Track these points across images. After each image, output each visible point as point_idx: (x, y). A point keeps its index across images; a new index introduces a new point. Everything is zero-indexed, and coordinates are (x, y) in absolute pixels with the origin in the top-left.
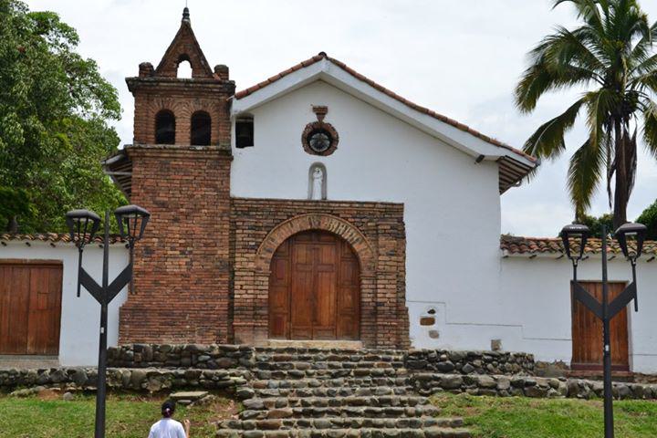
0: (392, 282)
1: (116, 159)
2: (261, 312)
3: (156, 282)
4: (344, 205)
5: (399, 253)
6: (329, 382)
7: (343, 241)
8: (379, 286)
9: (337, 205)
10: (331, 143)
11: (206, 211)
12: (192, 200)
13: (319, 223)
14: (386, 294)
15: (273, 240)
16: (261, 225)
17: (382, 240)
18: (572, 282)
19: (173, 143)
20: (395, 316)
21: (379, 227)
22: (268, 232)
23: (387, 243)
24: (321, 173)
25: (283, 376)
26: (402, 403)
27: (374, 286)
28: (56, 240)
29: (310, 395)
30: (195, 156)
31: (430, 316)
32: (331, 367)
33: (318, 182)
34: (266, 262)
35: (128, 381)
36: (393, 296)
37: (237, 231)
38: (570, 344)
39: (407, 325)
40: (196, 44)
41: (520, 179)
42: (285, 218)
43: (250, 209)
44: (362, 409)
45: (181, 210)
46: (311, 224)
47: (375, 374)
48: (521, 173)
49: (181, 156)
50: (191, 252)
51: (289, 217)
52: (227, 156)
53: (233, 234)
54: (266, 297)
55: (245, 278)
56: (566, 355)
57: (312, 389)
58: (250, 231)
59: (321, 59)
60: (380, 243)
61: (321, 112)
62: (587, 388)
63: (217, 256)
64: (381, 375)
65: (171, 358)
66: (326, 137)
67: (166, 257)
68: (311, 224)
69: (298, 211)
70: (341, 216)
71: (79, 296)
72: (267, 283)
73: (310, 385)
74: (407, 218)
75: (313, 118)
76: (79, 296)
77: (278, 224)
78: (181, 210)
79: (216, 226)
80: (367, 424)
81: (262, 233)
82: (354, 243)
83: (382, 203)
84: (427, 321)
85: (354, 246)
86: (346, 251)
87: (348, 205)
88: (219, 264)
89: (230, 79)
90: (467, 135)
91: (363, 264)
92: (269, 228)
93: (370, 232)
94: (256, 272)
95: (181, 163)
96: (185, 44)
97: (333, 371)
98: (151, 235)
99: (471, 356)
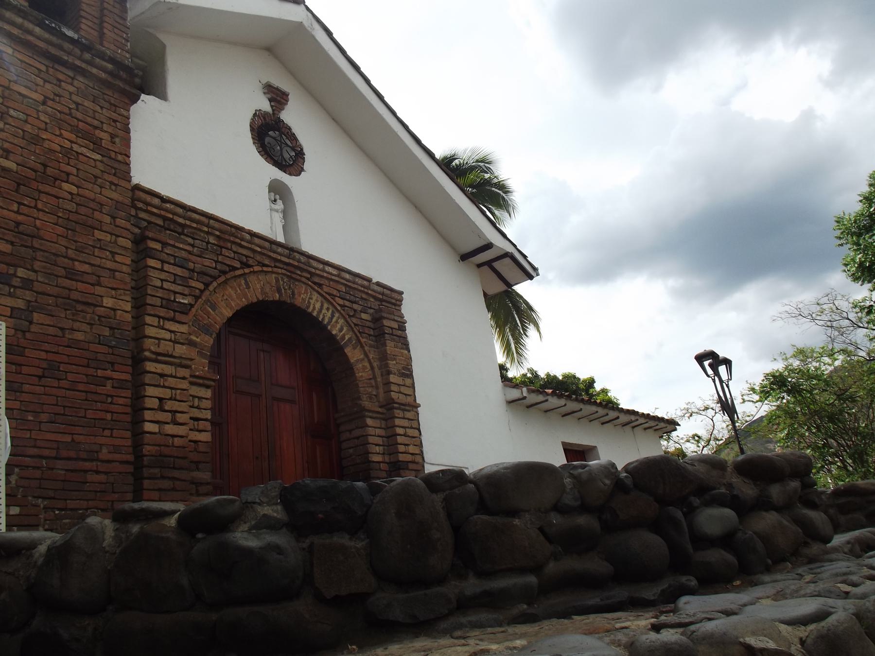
9: (321, 266)
11: (74, 189)
12: (32, 148)
13: (293, 293)
22: (207, 285)
24: (280, 202)
30: (53, 51)
34: (200, 353)
37: (151, 262)
42: (237, 265)
50: (27, 284)
54: (205, 437)
55: (171, 382)
58: (179, 271)
61: (278, 98)
63: (100, 311)
68: (279, 290)
69: (258, 258)
70: (326, 289)
72: (208, 404)
75: (265, 106)
79: (98, 234)
82: (346, 344)
83: (378, 284)
85: (348, 351)
87: (335, 272)
88: (107, 332)
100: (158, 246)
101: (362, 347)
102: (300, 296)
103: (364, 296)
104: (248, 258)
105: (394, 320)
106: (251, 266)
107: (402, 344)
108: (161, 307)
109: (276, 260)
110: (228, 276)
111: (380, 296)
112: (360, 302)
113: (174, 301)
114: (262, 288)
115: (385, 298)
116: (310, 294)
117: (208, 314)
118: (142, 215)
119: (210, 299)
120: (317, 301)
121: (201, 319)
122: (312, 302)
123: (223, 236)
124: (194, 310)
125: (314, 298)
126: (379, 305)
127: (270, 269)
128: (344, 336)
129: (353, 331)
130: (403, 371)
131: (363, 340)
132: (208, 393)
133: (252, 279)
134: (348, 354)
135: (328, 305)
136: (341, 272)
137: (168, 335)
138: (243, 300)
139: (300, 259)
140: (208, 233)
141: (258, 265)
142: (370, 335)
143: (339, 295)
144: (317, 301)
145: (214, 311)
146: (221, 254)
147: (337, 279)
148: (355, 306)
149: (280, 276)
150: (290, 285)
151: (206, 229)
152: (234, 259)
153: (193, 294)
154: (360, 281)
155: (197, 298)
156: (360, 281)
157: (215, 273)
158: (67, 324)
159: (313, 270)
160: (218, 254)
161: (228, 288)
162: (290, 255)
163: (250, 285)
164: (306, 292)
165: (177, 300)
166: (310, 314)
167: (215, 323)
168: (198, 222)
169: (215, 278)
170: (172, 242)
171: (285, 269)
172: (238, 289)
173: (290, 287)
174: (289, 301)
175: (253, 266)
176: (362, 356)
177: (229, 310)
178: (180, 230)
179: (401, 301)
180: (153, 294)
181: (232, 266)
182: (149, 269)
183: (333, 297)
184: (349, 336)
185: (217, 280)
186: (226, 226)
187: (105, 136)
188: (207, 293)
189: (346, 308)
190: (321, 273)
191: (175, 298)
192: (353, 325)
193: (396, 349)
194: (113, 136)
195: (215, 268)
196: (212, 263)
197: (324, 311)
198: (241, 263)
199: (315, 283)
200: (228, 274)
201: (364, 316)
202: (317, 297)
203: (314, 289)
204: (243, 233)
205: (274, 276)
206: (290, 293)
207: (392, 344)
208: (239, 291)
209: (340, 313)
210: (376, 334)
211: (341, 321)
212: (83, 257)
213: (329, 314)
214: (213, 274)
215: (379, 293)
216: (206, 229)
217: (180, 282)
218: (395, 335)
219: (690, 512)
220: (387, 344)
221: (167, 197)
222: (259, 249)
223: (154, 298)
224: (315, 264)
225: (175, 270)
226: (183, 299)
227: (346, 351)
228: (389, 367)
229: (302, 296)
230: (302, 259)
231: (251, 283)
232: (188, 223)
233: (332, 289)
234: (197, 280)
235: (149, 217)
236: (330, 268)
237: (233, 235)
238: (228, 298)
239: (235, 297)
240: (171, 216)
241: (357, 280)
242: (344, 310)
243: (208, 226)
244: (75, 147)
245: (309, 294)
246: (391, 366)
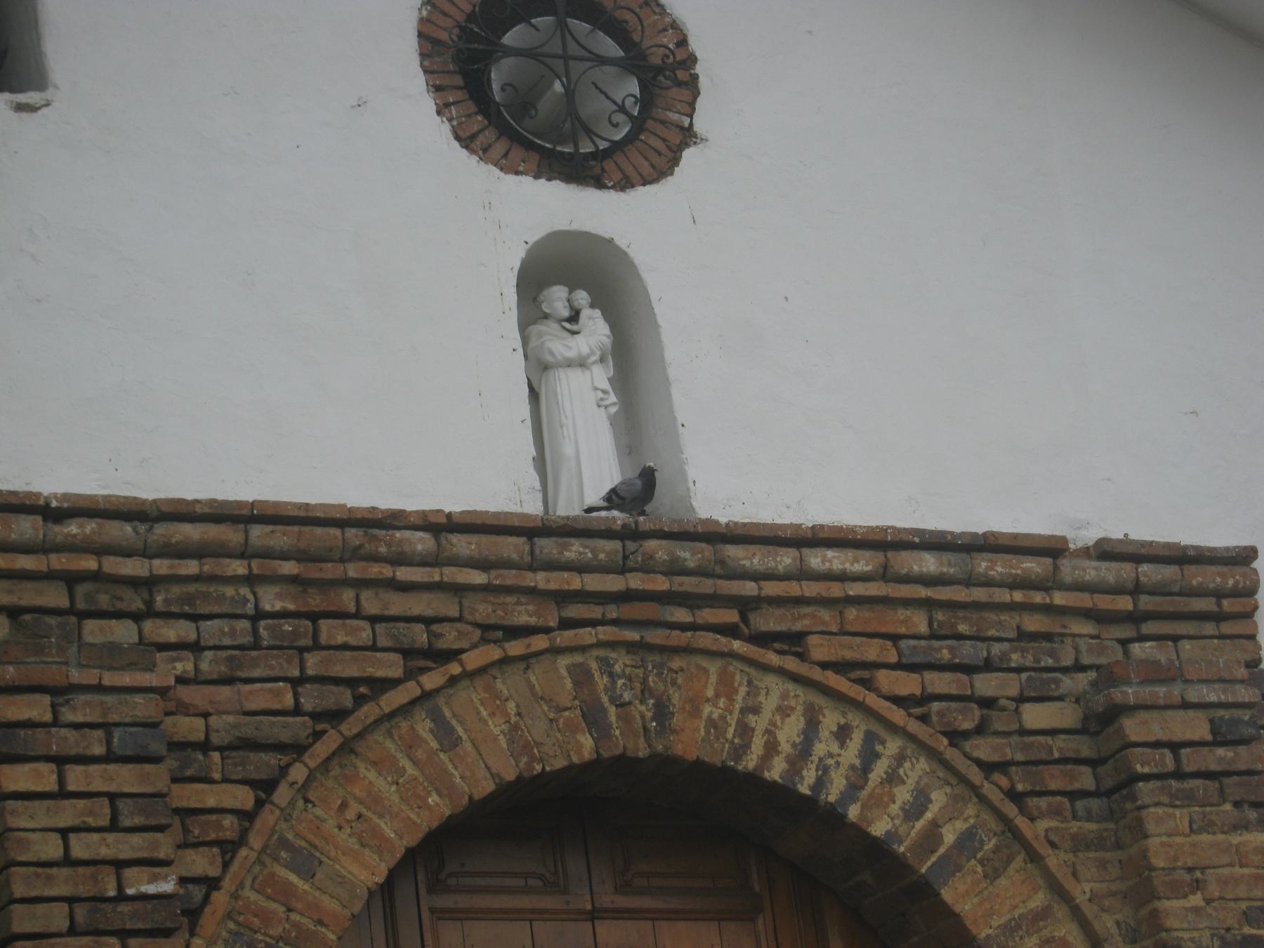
4: (834, 560)
9: (785, 559)
10: (647, 100)
13: (662, 712)
15: (306, 864)
16: (190, 728)
21: (1133, 728)
22: (266, 787)
46: (594, 719)
58: (125, 778)
60: (1159, 850)
66: (611, 48)
68: (594, 719)
69: (483, 610)
70: (819, 648)
81: (211, 797)
82: (950, 865)
83: (1106, 551)
87: (862, 563)
100: (36, 708)
101: (1034, 857)
102: (695, 713)
103: (1033, 623)
104: (435, 627)
105: (1185, 705)
106: (452, 655)
107: (1237, 804)
108: (73, 931)
109: (563, 597)
110: (350, 727)
111: (1124, 603)
112: (1014, 656)
113: (121, 897)
114: (515, 727)
115: (1147, 603)
116: (748, 693)
117: (286, 895)
119: (290, 836)
120: (784, 711)
121: (256, 922)
122: (758, 723)
123: (313, 571)
124: (220, 899)
125: (769, 704)
126: (1124, 643)
127: (540, 642)
128: (932, 835)
129: (982, 799)
130: (1247, 930)
131: (1035, 830)
133: (471, 697)
134: (957, 909)
135: (844, 714)
136: (890, 554)
138: (433, 799)
139: (674, 560)
140: (251, 580)
141: (484, 641)
142: (1073, 795)
143: (893, 659)
144: (784, 711)
145: (309, 876)
146: (317, 646)
147: (873, 589)
148: (986, 684)
149: (595, 653)
150: (644, 681)
151: (238, 568)
152: (374, 648)
153: (213, 836)
154: (999, 567)
155: (229, 848)
156: (999, 567)
157: (298, 727)
159: (753, 584)
160: (302, 650)
161: (362, 770)
162: (625, 557)
163: (460, 730)
164: (726, 688)
165: (130, 891)
166: (753, 779)
167: (320, 922)
168: (199, 552)
169: (298, 749)
170: (90, 677)
171: (615, 622)
172: (404, 762)
173: (646, 691)
174: (643, 753)
175: (462, 651)
176: (1039, 900)
177: (369, 856)
178: (135, 602)
179: (1251, 592)
180: (34, 893)
181: (371, 681)
182: (10, 804)
183: (865, 674)
184: (960, 826)
185: (306, 758)
186: (319, 531)
188: (268, 817)
189: (936, 706)
190: (794, 589)
191: (120, 888)
192: (975, 775)
193: (1205, 837)
195: (297, 711)
196: (278, 694)
198: (407, 653)
199: (763, 639)
200: (351, 719)
201: (1035, 716)
202: (785, 696)
203: (766, 668)
204: (398, 534)
205: (563, 662)
206: (649, 714)
207: (1181, 817)
208: (411, 770)
209: (911, 738)
210: (1109, 783)
211: (917, 770)
213: (851, 754)
214: (285, 736)
215: (1117, 591)
216: (238, 568)
217: (138, 820)
218: (1198, 775)
220: (1150, 827)
221: (66, 497)
222: (478, 578)
223: (40, 908)
224: (752, 558)
225: (111, 779)
226: (153, 879)
227: (947, 895)
228: (1167, 931)
229: (707, 709)
230: (687, 555)
231: (461, 723)
232: (161, 566)
233: (858, 640)
234: (225, 780)
235: (10, 592)
236: (830, 553)
237: (355, 554)
238: (364, 811)
239: (396, 798)
240: (90, 564)
241: (982, 564)
242: (924, 719)
243: (244, 554)
245: (743, 690)
246: (1171, 922)
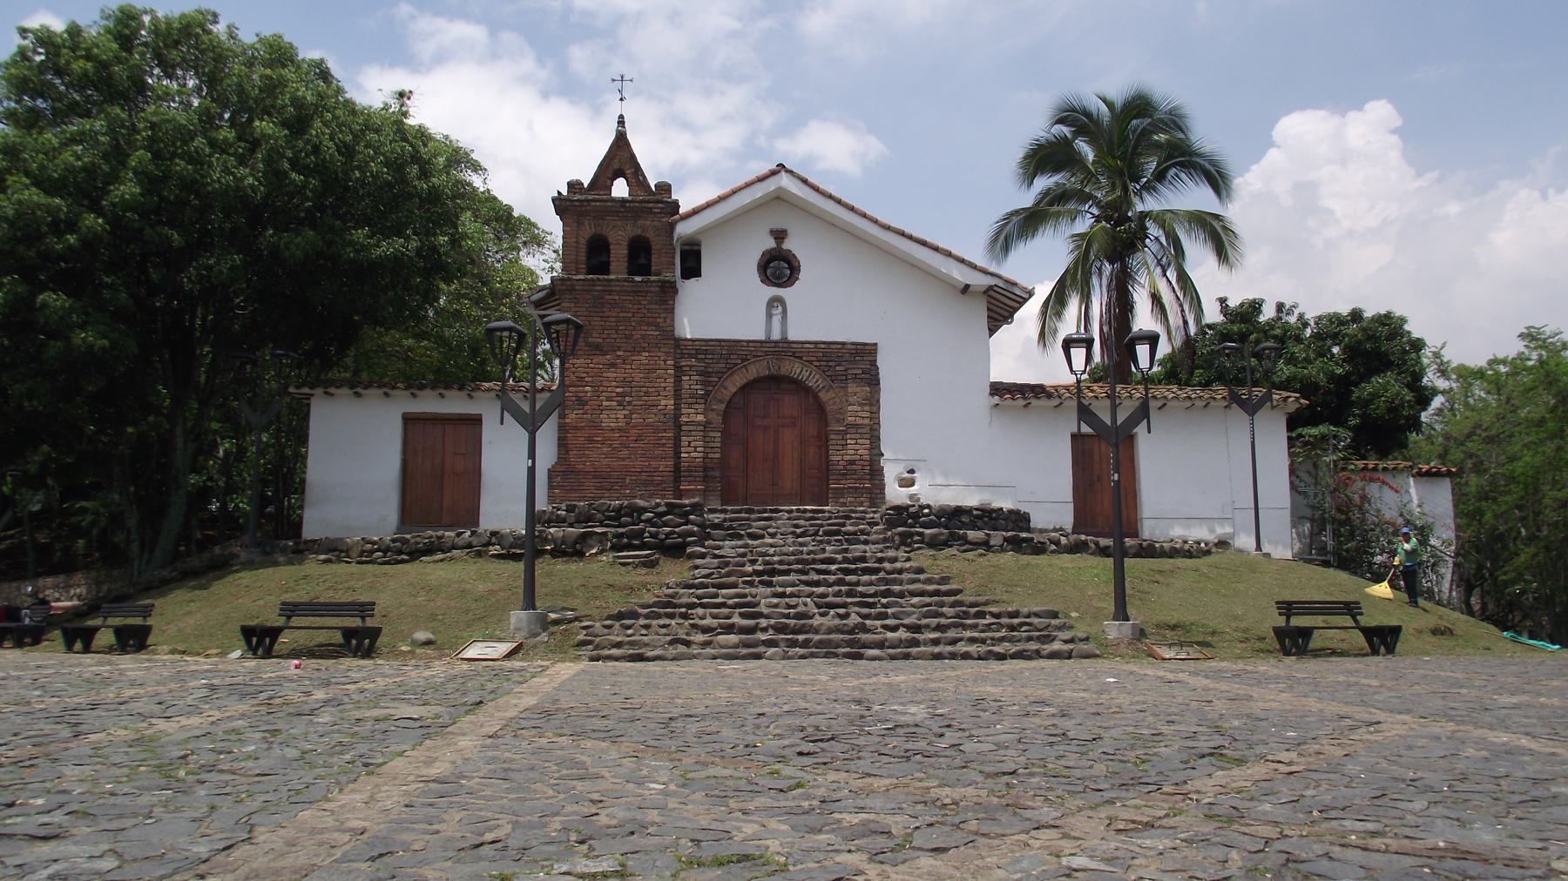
0: (865, 436)
1: (541, 295)
2: (712, 473)
3: (590, 440)
4: (808, 346)
5: (873, 403)
6: (794, 542)
7: (807, 390)
8: (849, 441)
9: (800, 346)
12: (631, 341)
14: (856, 449)
15: (726, 388)
16: (711, 370)
17: (852, 388)
18: (1073, 436)
19: (608, 274)
20: (868, 477)
21: (849, 372)
22: (720, 378)
23: (857, 391)
24: (780, 308)
25: (740, 537)
26: (880, 560)
27: (843, 442)
28: (473, 390)
29: (773, 555)
31: (906, 475)
32: (796, 526)
33: (776, 320)
34: (718, 414)
35: (559, 542)
36: (867, 452)
37: (684, 378)
38: (1071, 507)
39: (882, 487)
40: (633, 157)
41: (1011, 316)
42: (739, 361)
43: (698, 352)
44: (833, 567)
45: (619, 353)
46: (769, 369)
47: (846, 533)
48: (1011, 307)
49: (618, 288)
50: (629, 403)
51: (743, 361)
52: (668, 292)
53: (678, 381)
56: (1066, 518)
57: (773, 549)
58: (697, 378)
59: (779, 172)
60: (850, 390)
61: (780, 235)
62: (1093, 546)
64: (855, 533)
65: (609, 518)
67: (601, 409)
68: (769, 369)
69: (754, 353)
70: (804, 358)
71: (502, 423)
73: (772, 546)
74: (882, 362)
75: (771, 243)
76: (502, 423)
77: (731, 369)
78: (619, 353)
80: (840, 582)
83: (853, 344)
84: (907, 483)
85: (821, 395)
86: (811, 401)
89: (674, 197)
90: (951, 261)
91: (830, 417)
92: (720, 374)
93: (839, 378)
94: (706, 425)
95: (617, 297)
96: (620, 159)
97: (798, 531)
98: (584, 383)
99: (959, 511)
100: (688, 369)
118: (685, 351)
132: (719, 434)
137: (693, 411)
148: (830, 364)
155: (714, 387)
158: (646, 416)
187: (659, 320)
194: (665, 318)
197: (804, 372)
212: (651, 385)
219: (641, 514)
224: (795, 346)
241: (832, 346)
244: (648, 333)
